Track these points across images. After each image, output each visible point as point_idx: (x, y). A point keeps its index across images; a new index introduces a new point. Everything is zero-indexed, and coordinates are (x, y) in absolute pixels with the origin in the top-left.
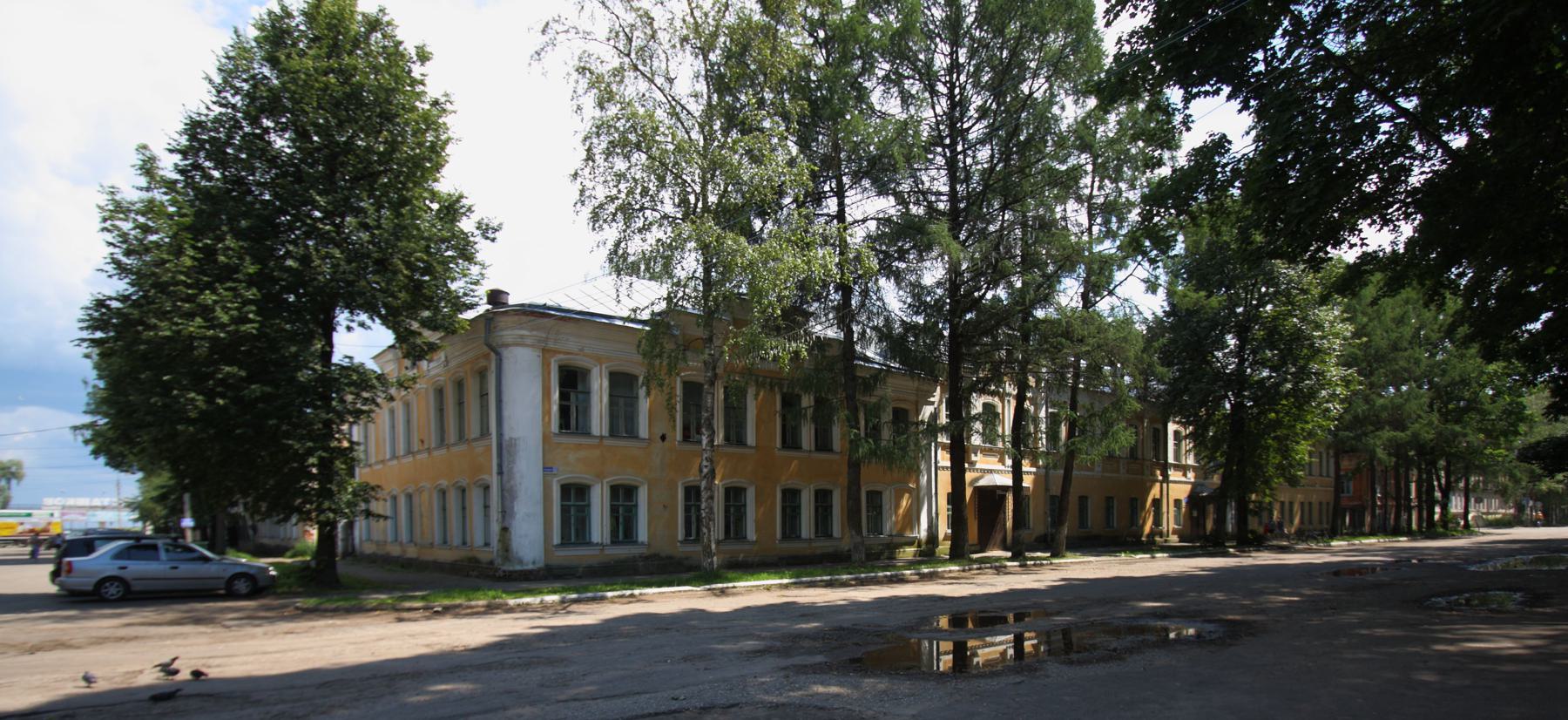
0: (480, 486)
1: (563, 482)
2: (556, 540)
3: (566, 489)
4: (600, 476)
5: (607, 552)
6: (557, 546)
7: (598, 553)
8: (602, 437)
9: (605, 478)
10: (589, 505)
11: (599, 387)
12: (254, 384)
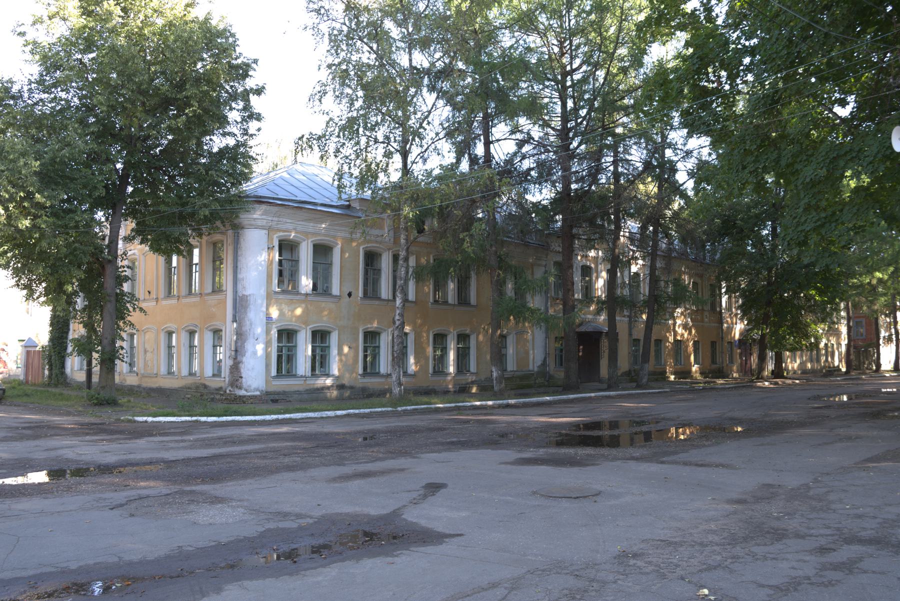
0: (210, 330)
1: (279, 328)
2: (274, 372)
3: (280, 332)
4: (306, 323)
5: (308, 382)
6: (274, 377)
7: (302, 382)
8: (454, 305)
9: (309, 325)
10: (296, 346)
11: (386, 263)
12: (647, 318)
